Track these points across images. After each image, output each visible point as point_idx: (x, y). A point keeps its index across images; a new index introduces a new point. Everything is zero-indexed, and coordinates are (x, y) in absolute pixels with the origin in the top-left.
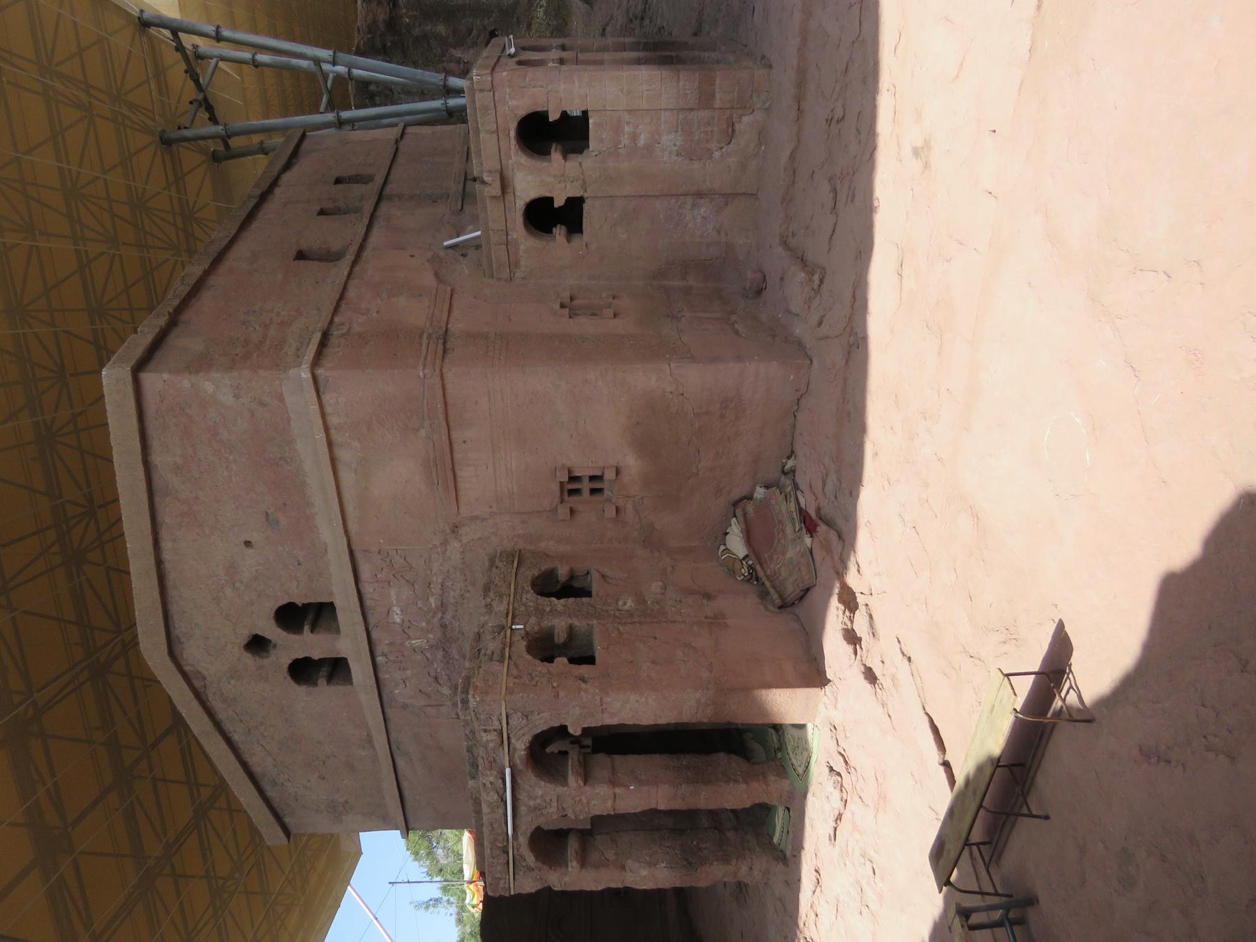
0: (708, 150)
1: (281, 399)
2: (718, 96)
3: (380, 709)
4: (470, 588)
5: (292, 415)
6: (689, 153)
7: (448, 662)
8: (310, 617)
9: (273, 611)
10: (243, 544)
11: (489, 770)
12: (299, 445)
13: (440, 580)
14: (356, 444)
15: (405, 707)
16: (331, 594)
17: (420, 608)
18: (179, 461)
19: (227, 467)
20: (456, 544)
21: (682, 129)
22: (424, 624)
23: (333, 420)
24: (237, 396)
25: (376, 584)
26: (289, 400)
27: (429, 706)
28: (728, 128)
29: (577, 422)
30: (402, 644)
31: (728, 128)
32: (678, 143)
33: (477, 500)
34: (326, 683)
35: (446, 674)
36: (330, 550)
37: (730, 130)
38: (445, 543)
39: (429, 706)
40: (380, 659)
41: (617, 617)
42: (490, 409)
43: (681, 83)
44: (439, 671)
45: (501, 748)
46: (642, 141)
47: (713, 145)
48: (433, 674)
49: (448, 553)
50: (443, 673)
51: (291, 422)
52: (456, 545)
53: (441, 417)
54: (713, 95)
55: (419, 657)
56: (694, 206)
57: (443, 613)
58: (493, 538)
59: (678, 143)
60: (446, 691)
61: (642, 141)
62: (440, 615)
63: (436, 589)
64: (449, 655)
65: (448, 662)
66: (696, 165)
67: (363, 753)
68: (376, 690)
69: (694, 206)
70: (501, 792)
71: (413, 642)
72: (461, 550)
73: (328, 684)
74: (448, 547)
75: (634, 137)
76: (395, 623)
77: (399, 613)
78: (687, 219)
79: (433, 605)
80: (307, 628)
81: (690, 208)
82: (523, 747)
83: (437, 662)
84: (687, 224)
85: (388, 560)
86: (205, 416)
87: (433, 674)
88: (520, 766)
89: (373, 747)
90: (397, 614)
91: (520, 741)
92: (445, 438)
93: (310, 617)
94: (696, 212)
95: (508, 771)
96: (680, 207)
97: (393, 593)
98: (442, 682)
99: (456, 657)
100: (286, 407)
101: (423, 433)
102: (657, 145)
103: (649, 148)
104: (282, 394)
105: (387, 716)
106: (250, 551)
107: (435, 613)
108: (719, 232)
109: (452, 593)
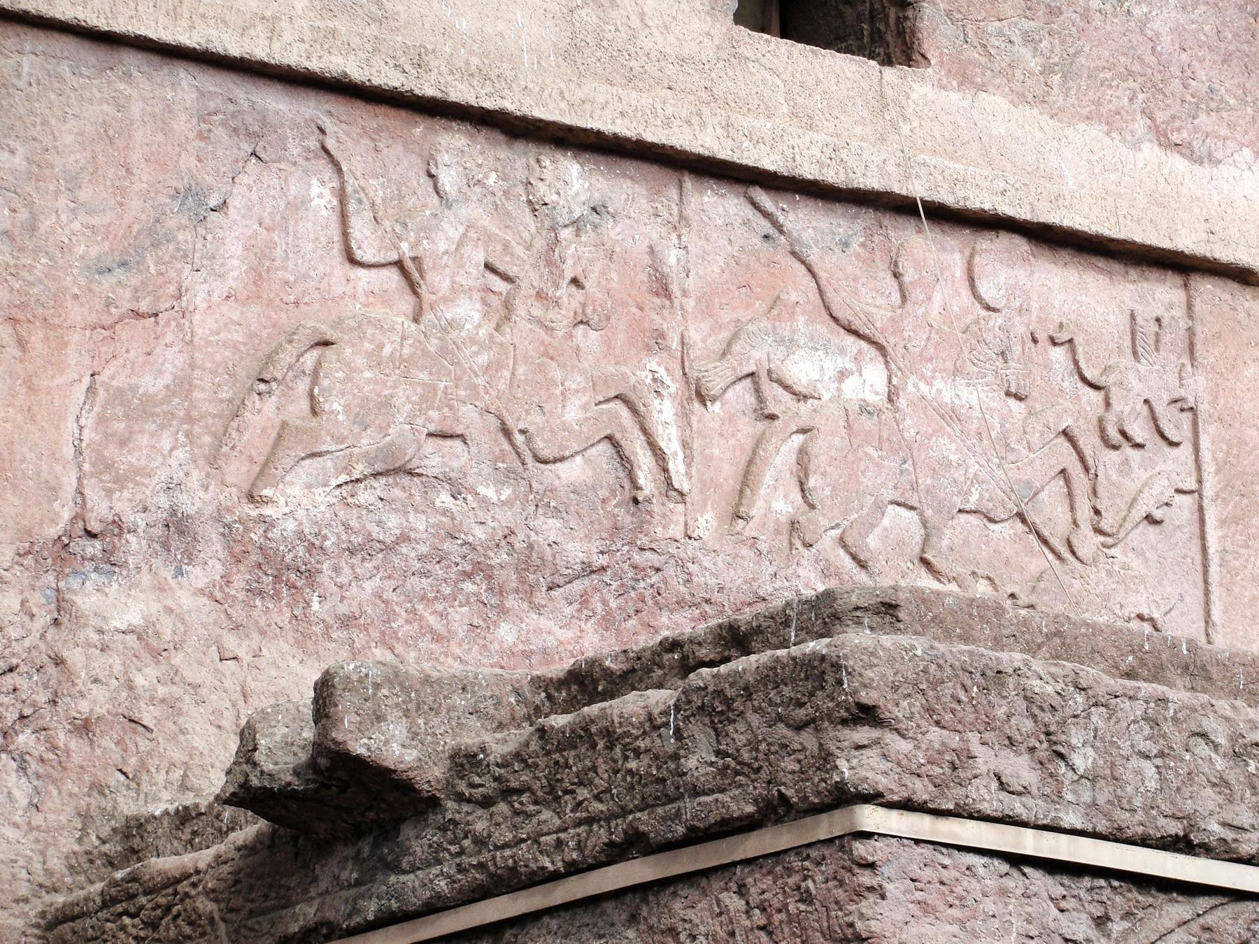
3: (234, 48)
7: (481, 569)
16: (964, 77)
17: (879, 508)
25: (1020, 329)
35: (404, 538)
36: (1179, 163)
44: (444, 499)
48: (435, 457)
50: (419, 523)
55: (572, 413)
64: (528, 592)
65: (481, 569)
68: (386, 77)
76: (790, 344)
77: (851, 388)
83: (507, 503)
87: (435, 457)
90: (842, 375)
98: (365, 496)
99: (506, 633)
105: (131, 59)
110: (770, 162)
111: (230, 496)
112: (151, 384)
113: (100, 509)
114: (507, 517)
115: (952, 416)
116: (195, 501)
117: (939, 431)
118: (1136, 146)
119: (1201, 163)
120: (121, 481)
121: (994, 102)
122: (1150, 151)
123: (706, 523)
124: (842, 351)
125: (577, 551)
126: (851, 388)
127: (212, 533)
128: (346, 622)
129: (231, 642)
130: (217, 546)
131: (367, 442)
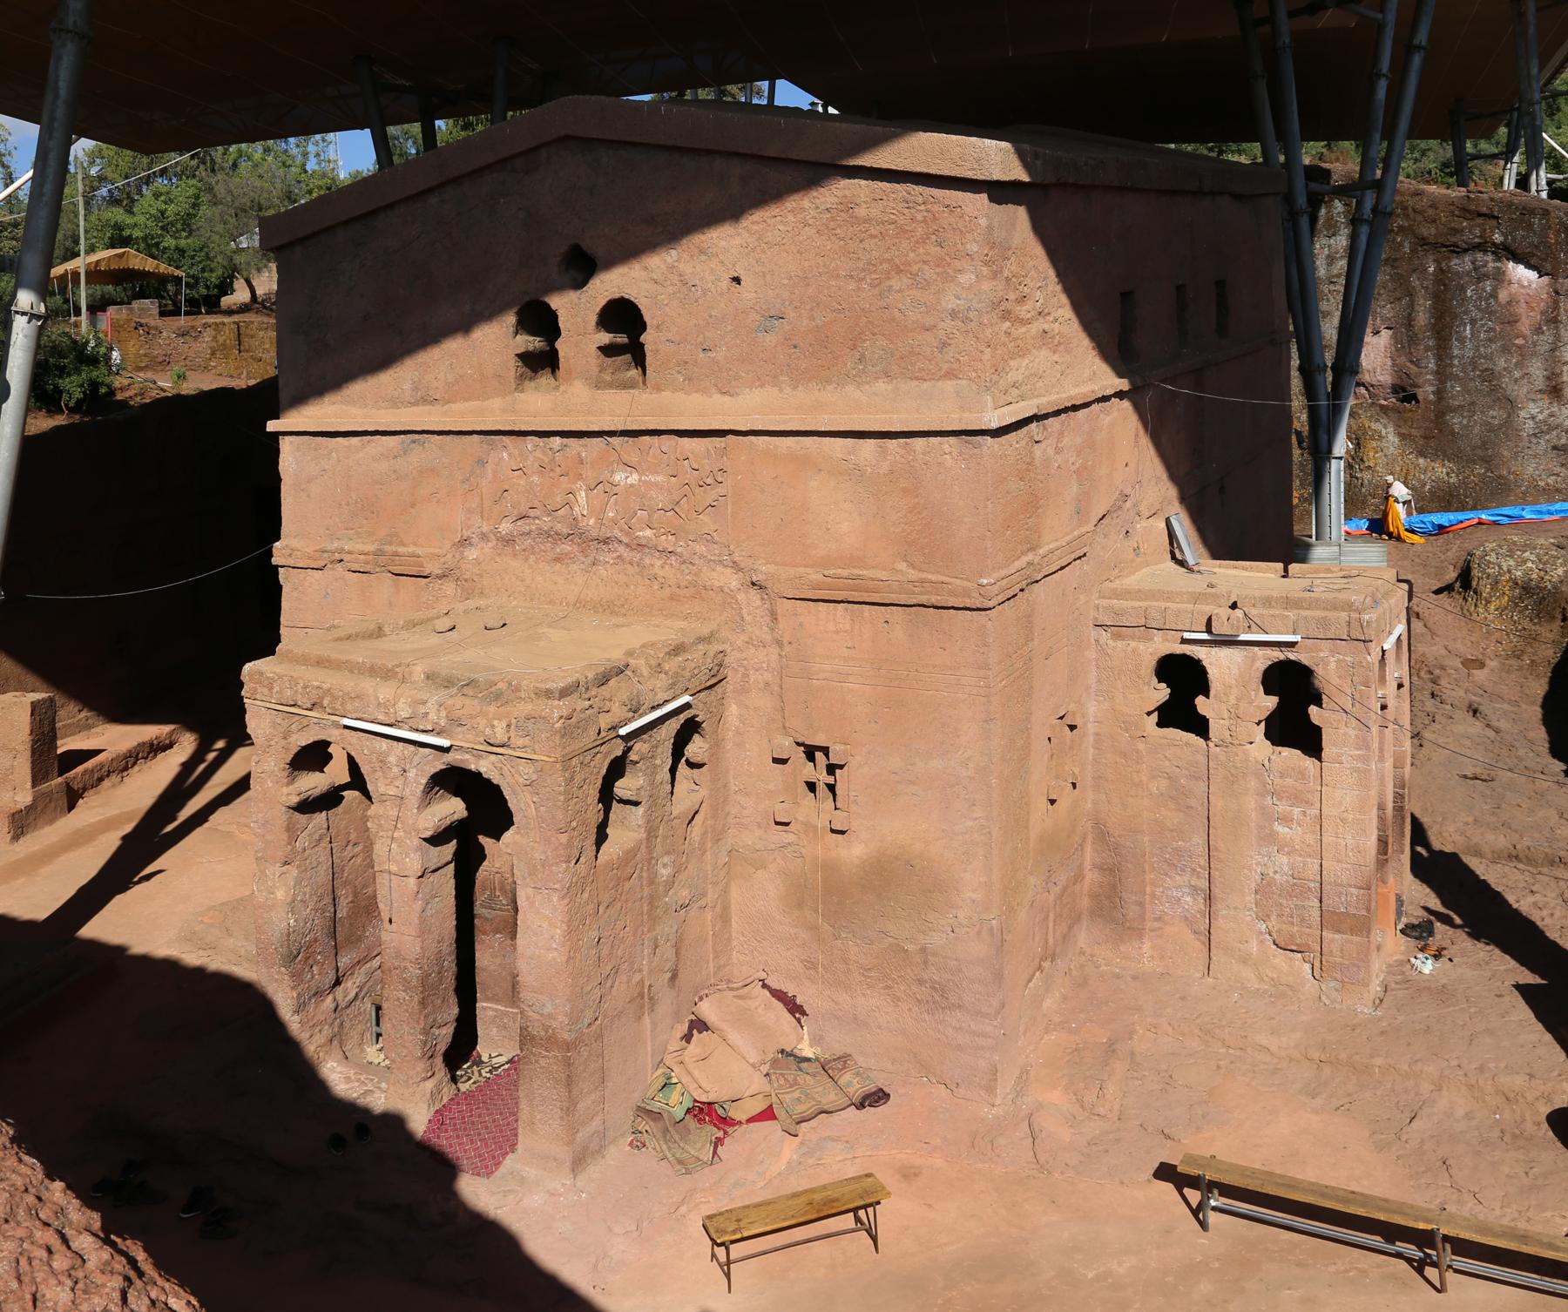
0: (1268, 916)
1: (951, 375)
2: (1337, 936)
3: (478, 428)
4: (667, 591)
5: (925, 385)
6: (1265, 888)
8: (622, 339)
9: (632, 299)
10: (736, 275)
11: (447, 716)
12: (881, 386)
13: (679, 550)
14: (885, 466)
15: (481, 463)
16: (658, 389)
18: (861, 212)
19: (852, 277)
20: (734, 584)
21: (1295, 884)
22: (611, 514)
23: (919, 443)
24: (954, 314)
26: (949, 386)
27: (482, 499)
28: (1297, 945)
29: (913, 783)
30: (580, 477)
31: (1297, 945)
32: (1277, 876)
33: (801, 625)
34: (519, 352)
35: (531, 531)
36: (727, 398)
37: (1294, 948)
38: (736, 566)
39: (482, 499)
40: (557, 441)
41: (650, 864)
42: (934, 666)
43: (1354, 891)
44: (537, 521)
45: (482, 740)
46: (1281, 829)
47: (1274, 923)
48: (532, 513)
49: (719, 568)
51: (915, 383)
52: (734, 583)
53: (923, 599)
54: (1339, 931)
55: (559, 499)
56: (1195, 889)
57: (627, 545)
58: (743, 637)
59: (1277, 876)
60: (505, 527)
61: (1281, 829)
62: (625, 540)
63: (667, 542)
64: (560, 539)
66: (1250, 899)
67: (407, 386)
69: (1195, 889)
70: (412, 723)
71: (583, 494)
72: (726, 590)
73: (517, 355)
74: (729, 570)
75: (1286, 819)
76: (613, 472)
77: (629, 481)
78: (1178, 878)
79: (641, 533)
80: (605, 338)
81: (1193, 883)
82: (482, 770)
84: (1170, 877)
85: (709, 481)
86: (925, 262)
87: (532, 513)
88: (453, 758)
89: (416, 404)
90: (627, 478)
91: (490, 766)
92: (893, 598)
93: (622, 339)
94: (1187, 890)
95: (445, 743)
96: (1194, 870)
97: (659, 478)
98: (519, 523)
100: (939, 380)
101: (903, 566)
102: (1276, 848)
103: (1270, 838)
104: (957, 378)
106: (725, 283)
107: (627, 534)
108: (1159, 919)
109: (659, 563)
110: (596, 428)
111: (492, 527)
112: (474, 506)
113: (466, 534)
114: (550, 524)
115: (656, 484)
116: (485, 529)
117: (651, 490)
118: (711, 397)
119: (732, 396)
120: (469, 528)
121: (666, 394)
122: (717, 397)
123: (592, 522)
124: (626, 471)
125: (565, 531)
126: (629, 481)
127: (491, 535)
128: (524, 550)
129: (498, 559)
130: (493, 538)
131: (516, 512)
